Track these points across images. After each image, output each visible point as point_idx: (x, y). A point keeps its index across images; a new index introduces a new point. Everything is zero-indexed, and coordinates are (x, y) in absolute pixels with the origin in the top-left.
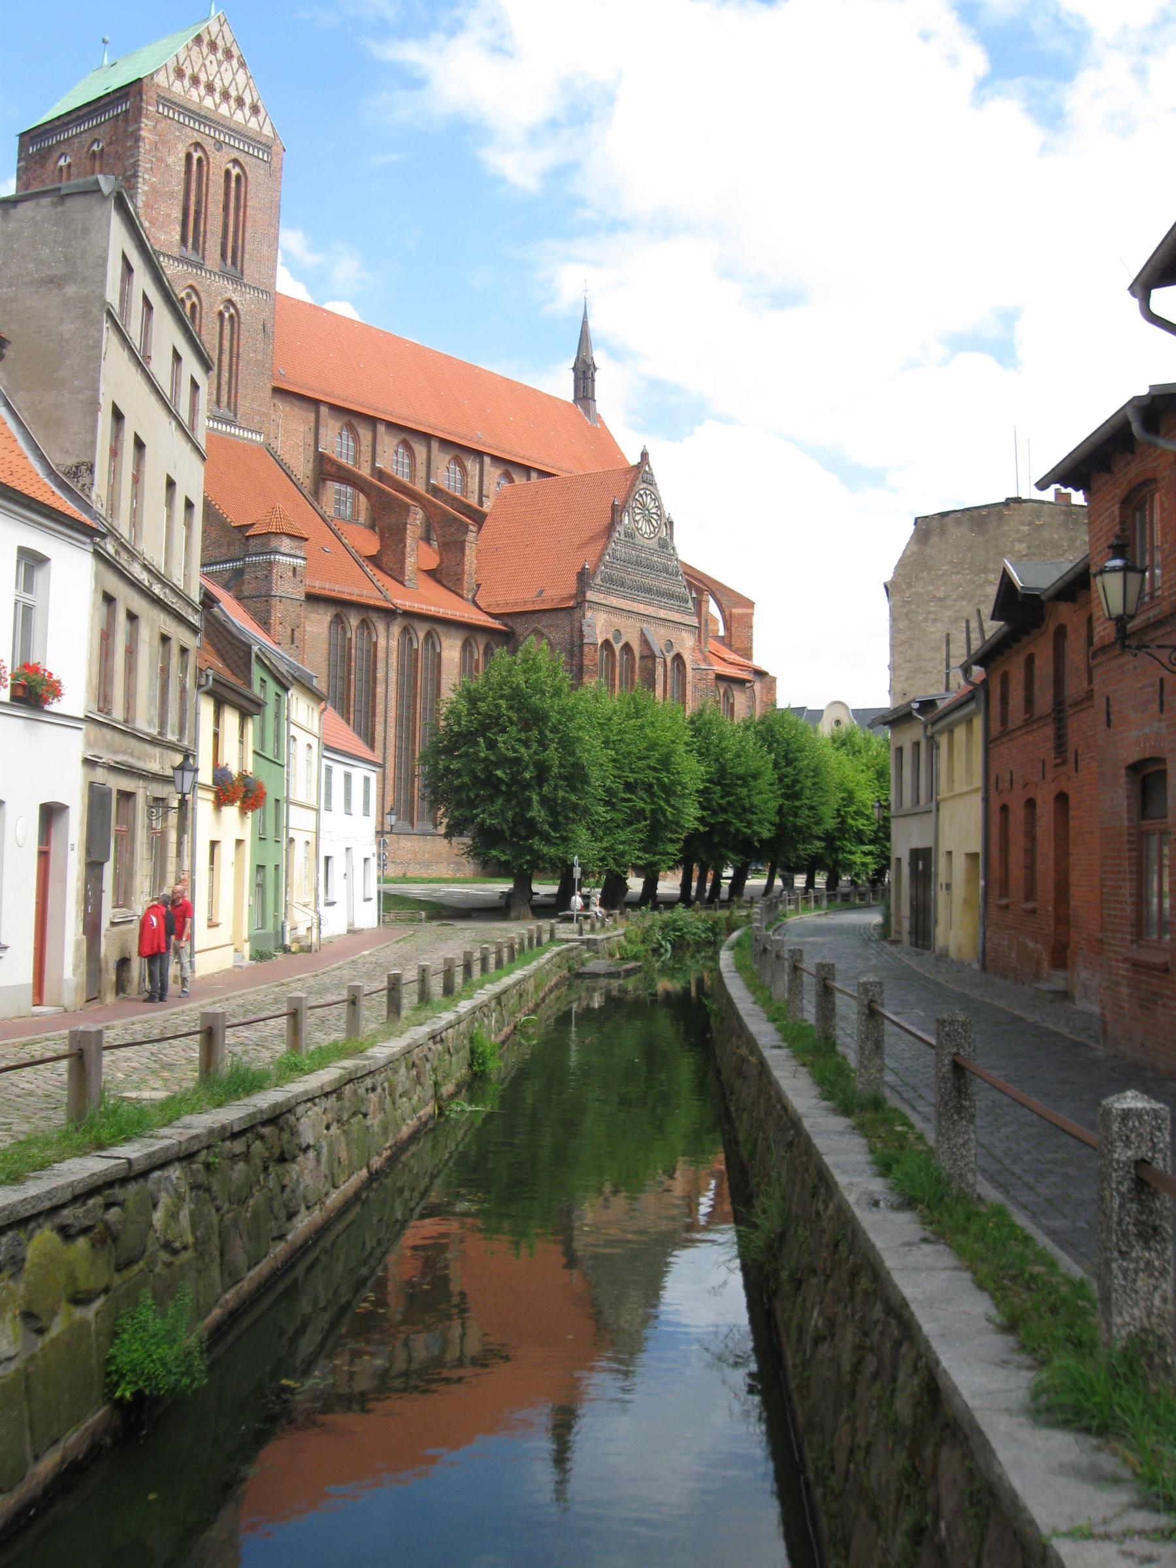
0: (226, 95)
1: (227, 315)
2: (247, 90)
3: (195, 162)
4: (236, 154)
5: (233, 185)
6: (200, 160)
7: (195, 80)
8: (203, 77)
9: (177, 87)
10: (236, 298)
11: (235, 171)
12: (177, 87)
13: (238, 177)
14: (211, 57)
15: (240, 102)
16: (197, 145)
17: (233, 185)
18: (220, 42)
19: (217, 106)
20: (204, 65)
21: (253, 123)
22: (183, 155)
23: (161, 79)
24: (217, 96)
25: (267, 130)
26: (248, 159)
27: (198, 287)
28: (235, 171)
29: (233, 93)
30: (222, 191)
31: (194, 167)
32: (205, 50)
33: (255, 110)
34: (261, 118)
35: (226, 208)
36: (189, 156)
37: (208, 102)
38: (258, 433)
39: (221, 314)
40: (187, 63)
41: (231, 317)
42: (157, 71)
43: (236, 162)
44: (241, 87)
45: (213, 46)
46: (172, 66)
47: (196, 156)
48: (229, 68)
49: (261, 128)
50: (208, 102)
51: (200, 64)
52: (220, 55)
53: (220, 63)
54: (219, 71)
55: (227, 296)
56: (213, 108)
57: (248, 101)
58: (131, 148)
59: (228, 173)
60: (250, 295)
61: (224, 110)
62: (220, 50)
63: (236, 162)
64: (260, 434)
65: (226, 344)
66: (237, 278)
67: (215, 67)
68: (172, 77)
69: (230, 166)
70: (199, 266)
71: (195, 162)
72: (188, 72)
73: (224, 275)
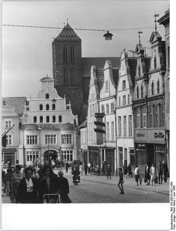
4: (72, 44)
5: (73, 49)
6: (66, 48)
9: (61, 39)
10: (74, 66)
14: (67, 32)
15: (72, 36)
19: (68, 39)
21: (76, 39)
25: (78, 39)
28: (73, 47)
42: (57, 38)
43: (73, 46)
44: (72, 34)
46: (60, 35)
47: (65, 47)
53: (68, 32)
54: (68, 33)
55: (72, 67)
57: (74, 36)
59: (71, 48)
61: (70, 39)
73: (72, 64)
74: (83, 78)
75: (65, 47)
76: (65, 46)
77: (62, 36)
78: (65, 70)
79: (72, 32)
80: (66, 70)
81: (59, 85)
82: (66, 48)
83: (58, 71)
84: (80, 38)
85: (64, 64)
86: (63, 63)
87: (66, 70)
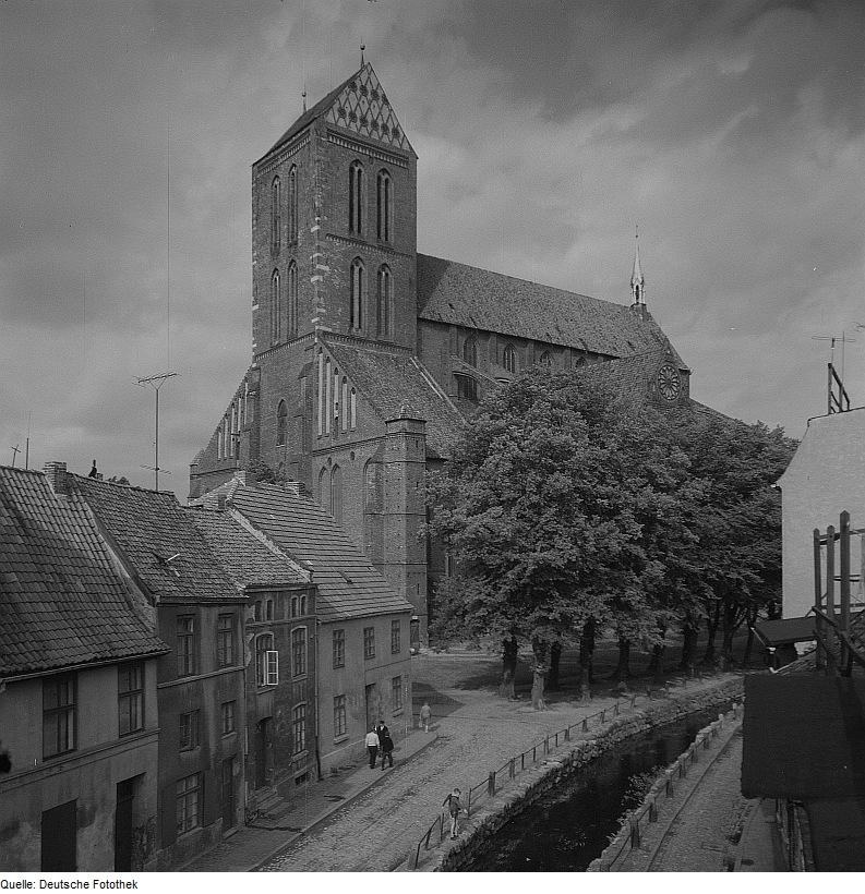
0: (375, 124)
3: (356, 174)
4: (385, 166)
5: (383, 186)
6: (360, 171)
7: (353, 116)
8: (358, 115)
9: (342, 123)
12: (342, 123)
13: (387, 180)
15: (385, 127)
16: (357, 162)
17: (383, 186)
18: (369, 88)
20: (358, 104)
21: (396, 144)
22: (347, 169)
23: (330, 118)
24: (369, 128)
25: (406, 147)
26: (394, 168)
27: (362, 257)
28: (384, 177)
29: (380, 123)
30: (376, 192)
31: (356, 177)
32: (359, 92)
33: (396, 132)
35: (379, 204)
36: (352, 170)
37: (364, 132)
39: (380, 273)
41: (387, 274)
43: (384, 171)
45: (364, 89)
47: (357, 169)
49: (401, 145)
50: (364, 132)
52: (369, 97)
56: (367, 134)
58: (313, 168)
61: (375, 136)
63: (384, 171)
65: (383, 292)
66: (387, 249)
70: (364, 243)
71: (356, 174)
72: (348, 111)
74: (420, 320)
75: (357, 169)
76: (357, 162)
78: (352, 268)
79: (386, 112)
81: (330, 330)
82: (360, 171)
83: (327, 268)
84: (411, 148)
85: (351, 241)
86: (346, 235)
87: (357, 269)
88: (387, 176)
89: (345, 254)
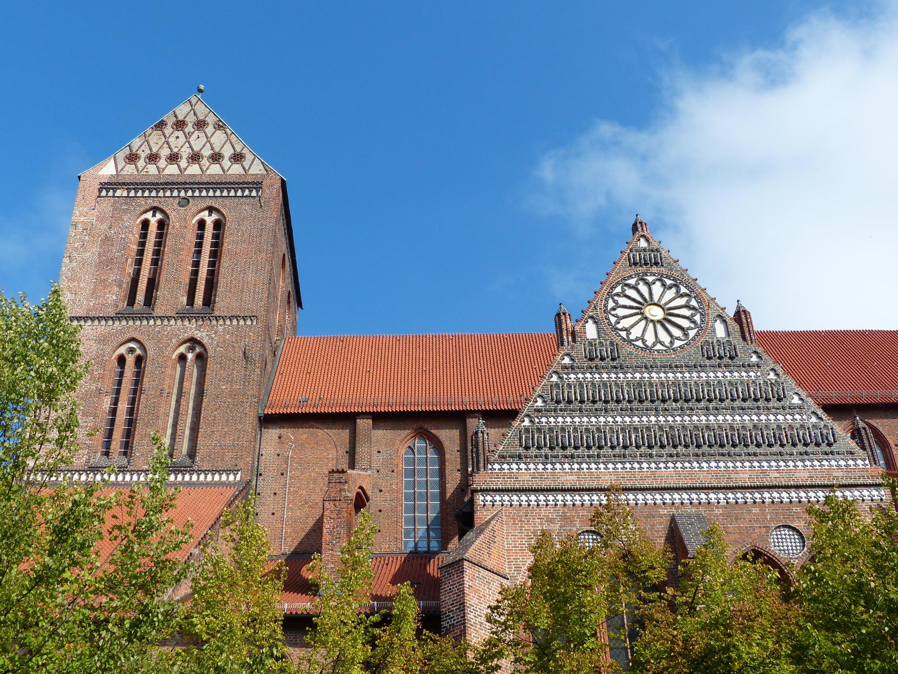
1: (190, 356)
2: (228, 145)
4: (209, 202)
10: (198, 335)
11: (210, 220)
26: (227, 202)
34: (246, 164)
38: (228, 471)
40: (143, 148)
43: (211, 209)
48: (202, 135)
51: (160, 144)
53: (188, 136)
60: (220, 326)
62: (190, 125)
64: (235, 471)
67: (182, 139)
68: (121, 164)
69: (205, 215)
77: (143, 155)
80: (130, 359)
87: (130, 359)
88: (215, 216)
89: (102, 340)
